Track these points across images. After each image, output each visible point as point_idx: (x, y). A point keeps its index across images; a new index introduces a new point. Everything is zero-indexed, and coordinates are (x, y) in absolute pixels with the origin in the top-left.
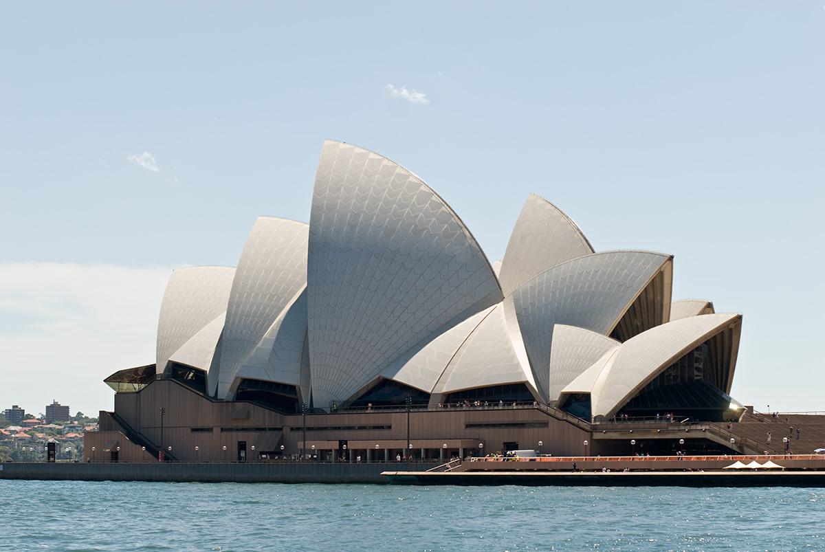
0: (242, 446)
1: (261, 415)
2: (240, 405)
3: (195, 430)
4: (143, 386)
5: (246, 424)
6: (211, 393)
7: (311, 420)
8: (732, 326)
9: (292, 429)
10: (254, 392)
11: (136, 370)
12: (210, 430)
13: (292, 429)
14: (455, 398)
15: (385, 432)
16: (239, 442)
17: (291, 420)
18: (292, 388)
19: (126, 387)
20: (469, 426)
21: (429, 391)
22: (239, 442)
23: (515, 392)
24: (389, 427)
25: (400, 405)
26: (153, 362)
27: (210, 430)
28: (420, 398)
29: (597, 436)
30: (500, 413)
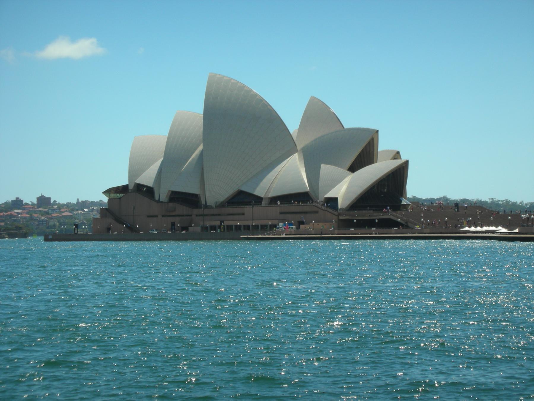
0: (173, 224)
1: (181, 209)
2: (171, 205)
3: (148, 216)
4: (122, 195)
5: (174, 214)
6: (157, 198)
7: (206, 211)
8: (404, 165)
9: (197, 215)
10: (177, 197)
11: (117, 188)
12: (156, 216)
13: (197, 215)
14: (273, 200)
15: (241, 217)
16: (172, 223)
17: (195, 211)
18: (196, 196)
19: (113, 195)
20: (281, 213)
21: (262, 196)
22: (172, 223)
23: (303, 197)
24: (243, 214)
25: (248, 203)
26: (127, 183)
27: (156, 216)
28: (258, 200)
29: (341, 218)
30: (296, 207)
